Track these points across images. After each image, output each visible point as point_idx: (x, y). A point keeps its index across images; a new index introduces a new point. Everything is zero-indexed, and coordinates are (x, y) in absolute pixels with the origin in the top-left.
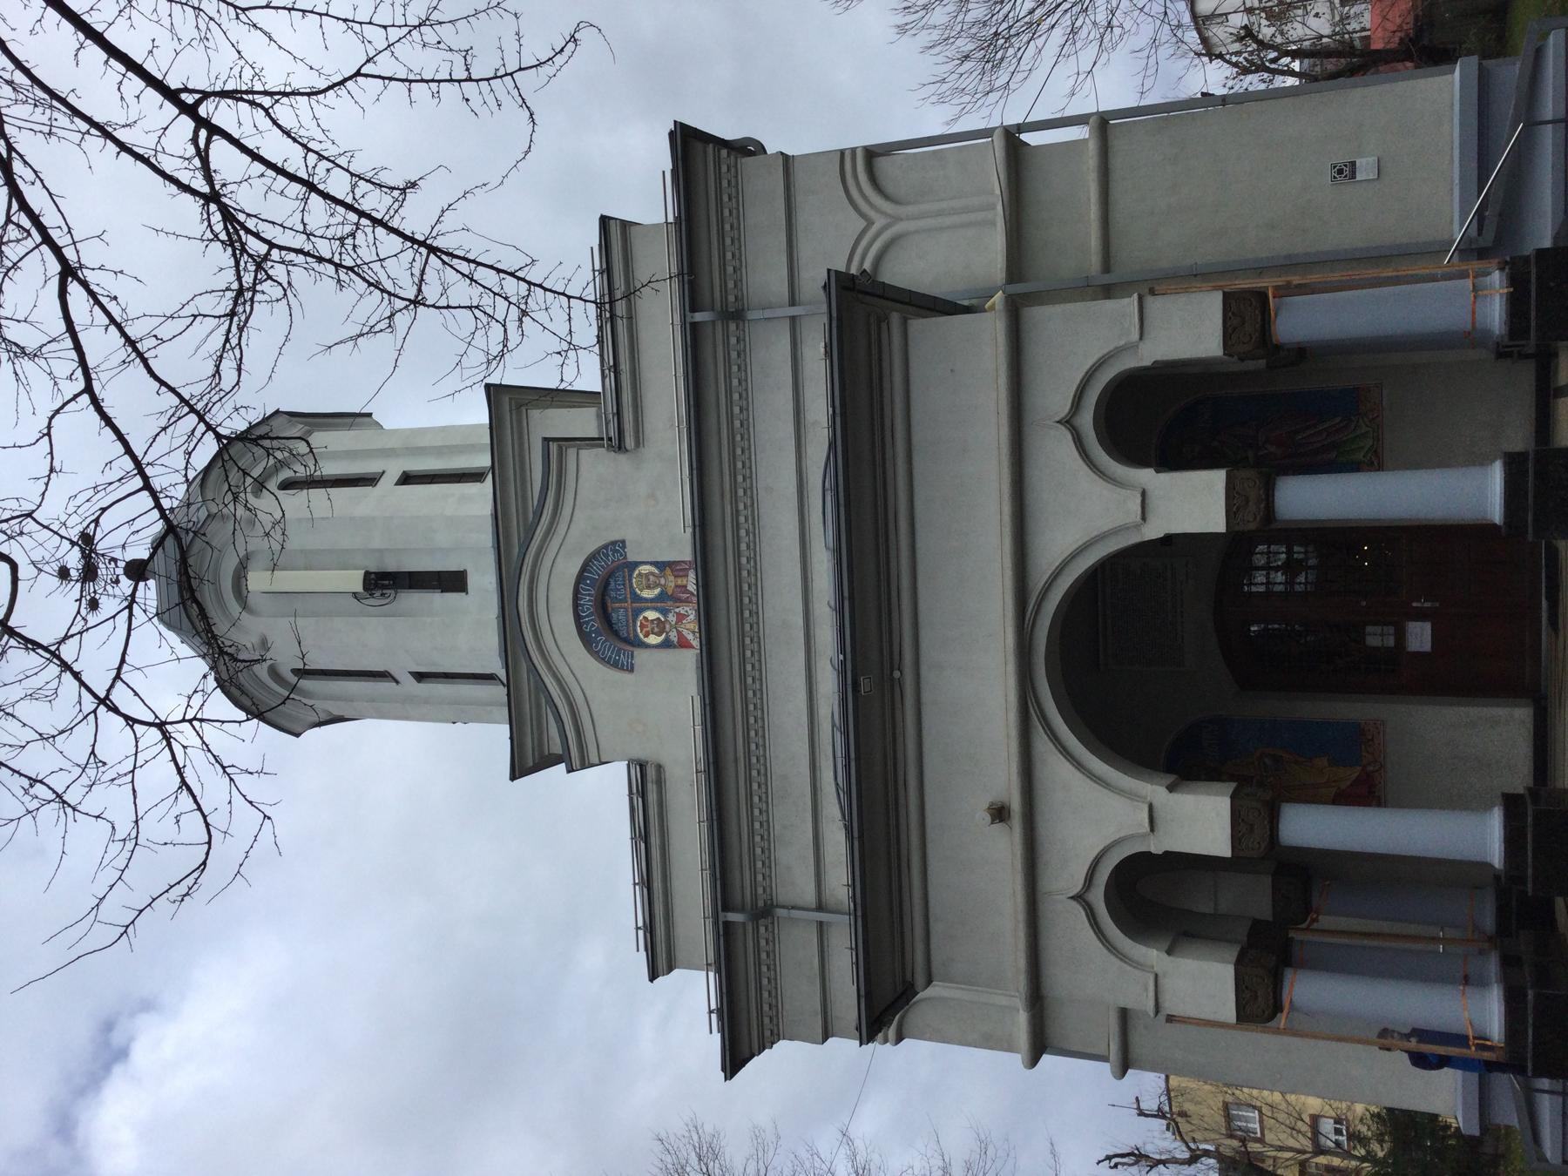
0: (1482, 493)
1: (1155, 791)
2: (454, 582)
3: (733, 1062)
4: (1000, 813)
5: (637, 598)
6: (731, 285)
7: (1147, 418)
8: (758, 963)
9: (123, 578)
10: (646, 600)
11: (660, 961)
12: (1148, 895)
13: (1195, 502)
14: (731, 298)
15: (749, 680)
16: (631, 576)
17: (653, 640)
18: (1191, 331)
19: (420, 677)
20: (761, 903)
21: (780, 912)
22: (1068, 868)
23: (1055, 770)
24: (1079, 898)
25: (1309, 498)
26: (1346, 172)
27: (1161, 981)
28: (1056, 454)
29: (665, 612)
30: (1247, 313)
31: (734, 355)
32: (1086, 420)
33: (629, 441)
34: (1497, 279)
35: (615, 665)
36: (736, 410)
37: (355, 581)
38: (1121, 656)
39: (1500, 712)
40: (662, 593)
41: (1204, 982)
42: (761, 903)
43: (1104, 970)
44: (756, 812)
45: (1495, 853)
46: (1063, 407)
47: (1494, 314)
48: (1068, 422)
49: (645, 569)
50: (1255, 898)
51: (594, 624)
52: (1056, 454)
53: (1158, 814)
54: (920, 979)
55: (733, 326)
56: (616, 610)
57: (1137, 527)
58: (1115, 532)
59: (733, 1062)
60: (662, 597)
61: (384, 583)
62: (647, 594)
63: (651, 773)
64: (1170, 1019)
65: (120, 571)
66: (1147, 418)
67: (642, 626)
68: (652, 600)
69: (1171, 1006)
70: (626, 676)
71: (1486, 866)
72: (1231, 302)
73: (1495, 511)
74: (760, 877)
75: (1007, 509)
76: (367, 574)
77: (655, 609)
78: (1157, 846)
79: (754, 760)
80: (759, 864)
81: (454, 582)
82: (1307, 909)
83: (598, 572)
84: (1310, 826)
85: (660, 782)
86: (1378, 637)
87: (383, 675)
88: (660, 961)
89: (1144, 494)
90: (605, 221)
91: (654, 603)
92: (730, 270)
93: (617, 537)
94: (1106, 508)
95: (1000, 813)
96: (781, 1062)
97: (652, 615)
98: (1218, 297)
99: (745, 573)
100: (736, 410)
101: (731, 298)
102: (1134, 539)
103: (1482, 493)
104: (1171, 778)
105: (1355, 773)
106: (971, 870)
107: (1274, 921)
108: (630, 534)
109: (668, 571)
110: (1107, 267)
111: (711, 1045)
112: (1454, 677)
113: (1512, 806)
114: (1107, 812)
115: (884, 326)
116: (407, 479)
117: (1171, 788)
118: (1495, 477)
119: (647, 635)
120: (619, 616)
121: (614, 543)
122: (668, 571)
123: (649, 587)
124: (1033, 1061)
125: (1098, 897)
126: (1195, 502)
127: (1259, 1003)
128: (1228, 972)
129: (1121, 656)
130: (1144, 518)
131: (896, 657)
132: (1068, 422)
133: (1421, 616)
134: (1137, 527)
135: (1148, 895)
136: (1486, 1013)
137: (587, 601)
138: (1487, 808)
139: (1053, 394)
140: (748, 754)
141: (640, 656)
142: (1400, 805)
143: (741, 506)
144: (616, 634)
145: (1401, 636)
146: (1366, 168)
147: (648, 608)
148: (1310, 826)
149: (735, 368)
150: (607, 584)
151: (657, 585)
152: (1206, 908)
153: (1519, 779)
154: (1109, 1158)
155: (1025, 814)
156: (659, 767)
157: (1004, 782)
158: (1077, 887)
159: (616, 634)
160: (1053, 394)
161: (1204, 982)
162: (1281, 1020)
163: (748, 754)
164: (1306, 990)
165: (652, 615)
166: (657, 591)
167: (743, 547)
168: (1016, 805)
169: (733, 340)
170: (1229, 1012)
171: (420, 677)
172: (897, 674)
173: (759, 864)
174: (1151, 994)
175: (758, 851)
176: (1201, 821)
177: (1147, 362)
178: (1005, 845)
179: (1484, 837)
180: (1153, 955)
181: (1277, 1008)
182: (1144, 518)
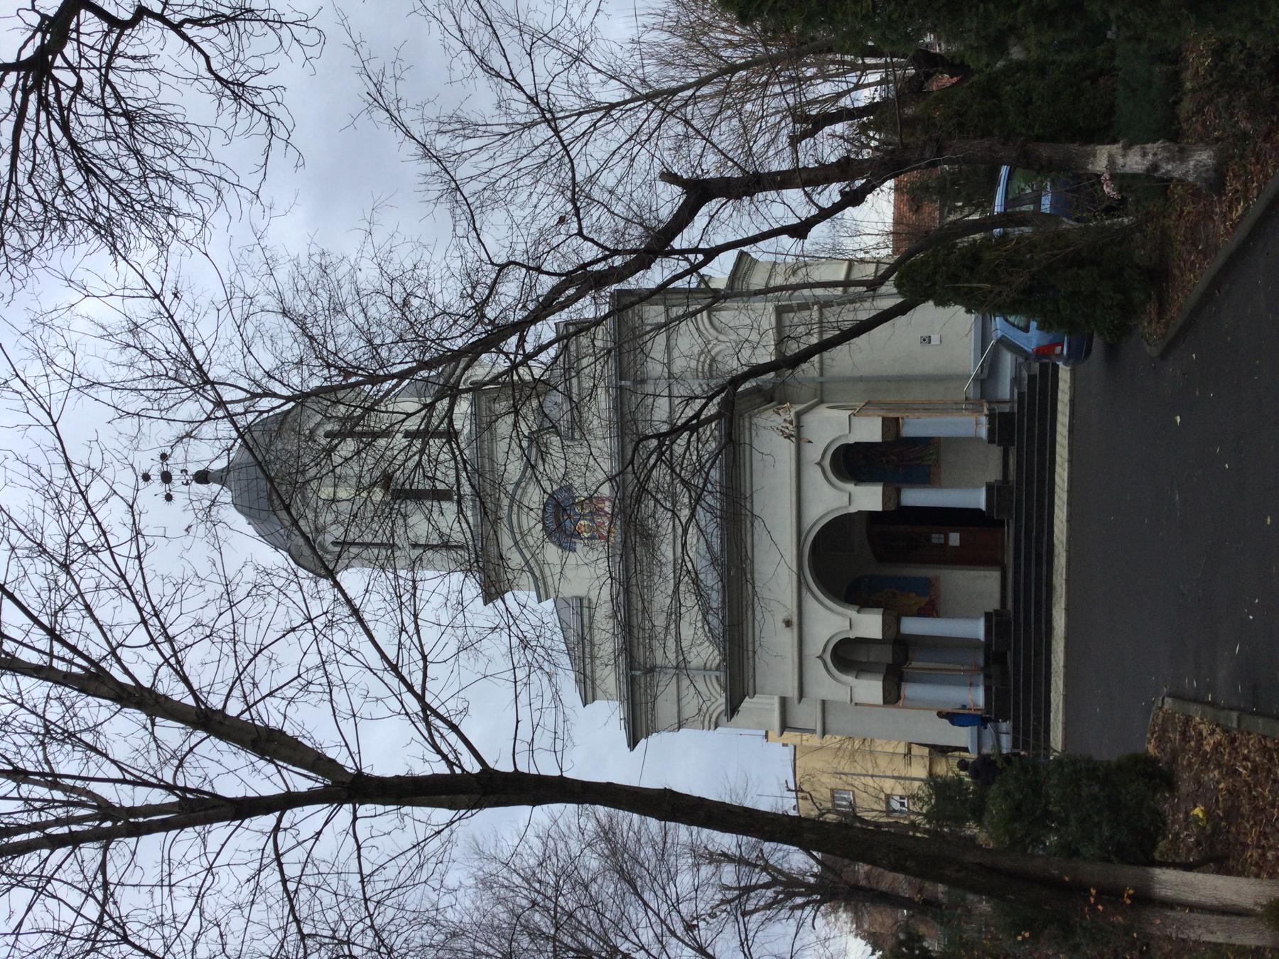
0: (978, 499)
1: (852, 613)
3: (633, 742)
7: (851, 462)
11: (588, 694)
12: (847, 656)
13: (869, 498)
18: (869, 430)
23: (811, 605)
24: (820, 657)
25: (914, 497)
26: (927, 340)
28: (814, 477)
30: (891, 425)
32: (827, 463)
34: (984, 420)
38: (837, 560)
39: (987, 573)
43: (829, 685)
47: (983, 432)
48: (819, 464)
50: (886, 656)
52: (814, 477)
54: (751, 692)
58: (837, 509)
59: (633, 742)
63: (586, 603)
66: (851, 462)
69: (856, 700)
72: (884, 420)
73: (983, 506)
78: (852, 636)
82: (907, 659)
84: (913, 626)
86: (937, 539)
88: (588, 694)
94: (834, 498)
96: (653, 743)
98: (880, 419)
105: (927, 599)
106: (775, 646)
107: (897, 663)
110: (821, 375)
111: (622, 736)
112: (967, 558)
113: (988, 616)
114: (832, 622)
124: (782, 734)
125: (828, 657)
126: (869, 498)
127: (892, 696)
128: (880, 684)
129: (837, 560)
132: (819, 464)
135: (847, 656)
136: (976, 697)
138: (978, 618)
139: (814, 453)
142: (948, 617)
145: (947, 539)
146: (935, 340)
148: (913, 626)
152: (864, 660)
153: (994, 604)
155: (798, 624)
160: (814, 453)
161: (870, 689)
162: (901, 703)
164: (909, 690)
168: (795, 620)
170: (881, 701)
176: (870, 625)
177: (852, 442)
179: (977, 629)
180: (850, 679)
181: (899, 698)
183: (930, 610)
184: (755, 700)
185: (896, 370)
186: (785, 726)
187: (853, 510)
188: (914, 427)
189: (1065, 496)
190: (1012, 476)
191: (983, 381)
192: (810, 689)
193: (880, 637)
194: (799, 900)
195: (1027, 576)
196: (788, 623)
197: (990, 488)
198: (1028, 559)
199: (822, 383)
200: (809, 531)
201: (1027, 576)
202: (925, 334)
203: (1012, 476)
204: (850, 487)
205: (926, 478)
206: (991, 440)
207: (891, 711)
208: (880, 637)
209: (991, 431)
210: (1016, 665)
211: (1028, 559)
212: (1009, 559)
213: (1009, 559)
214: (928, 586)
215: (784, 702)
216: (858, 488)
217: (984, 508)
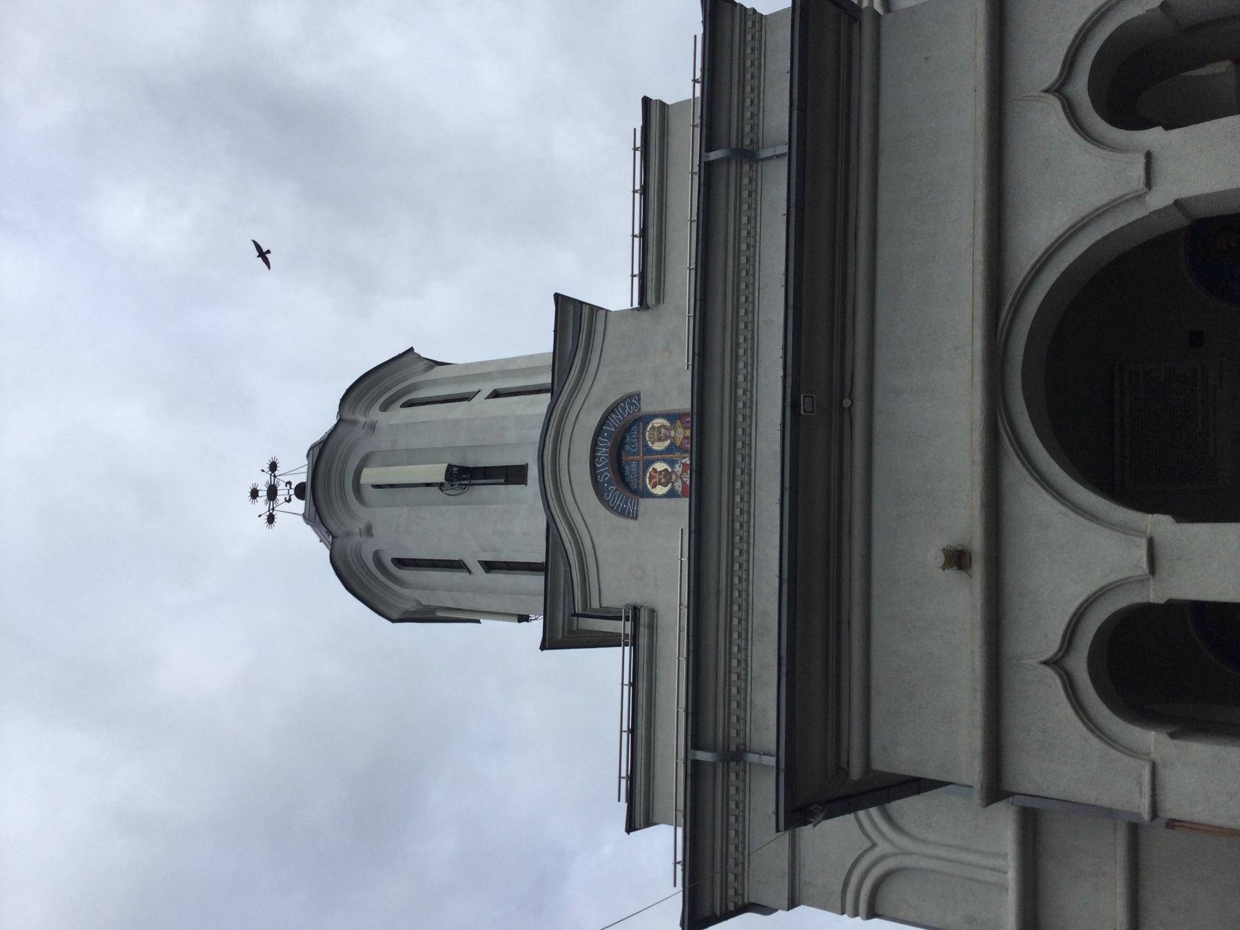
2: (515, 475)
4: (957, 559)
5: (650, 451)
6: (747, 128)
8: (726, 812)
9: (294, 498)
10: (657, 452)
14: (747, 142)
15: (737, 512)
16: (645, 429)
17: (660, 490)
19: (489, 566)
20: (733, 748)
21: (752, 758)
22: (1040, 630)
24: (1055, 663)
27: (1163, 773)
28: (1044, 127)
29: (672, 463)
31: (745, 194)
32: (1080, 87)
33: (651, 298)
35: (623, 513)
36: (744, 247)
37: (437, 473)
40: (672, 444)
42: (733, 748)
44: (735, 649)
46: (1052, 71)
48: (1059, 89)
49: (658, 422)
51: (607, 474)
53: (1162, 552)
55: (746, 167)
56: (629, 463)
57: (1139, 197)
60: (669, 450)
61: (463, 476)
62: (658, 446)
63: (644, 618)
64: (1172, 824)
65: (292, 492)
67: (651, 477)
68: (661, 452)
69: (1173, 807)
70: (631, 523)
74: (734, 719)
75: (981, 196)
76: (450, 467)
77: (664, 460)
79: (736, 594)
80: (734, 705)
81: (515, 475)
83: (616, 422)
85: (652, 627)
87: (457, 565)
89: (1149, 156)
90: (646, 101)
91: (665, 455)
92: (748, 115)
93: (631, 389)
95: (957, 559)
97: (660, 466)
99: (740, 405)
100: (744, 247)
101: (747, 142)
102: (1136, 213)
106: (925, 637)
108: (644, 385)
109: (678, 423)
114: (1091, 554)
115: (856, 26)
116: (496, 394)
119: (654, 487)
120: (631, 468)
121: (631, 396)
122: (678, 423)
123: (660, 440)
125: (1079, 664)
130: (1149, 182)
131: (848, 387)
132: (1059, 89)
134: (1139, 197)
137: (603, 453)
140: (730, 585)
141: (645, 503)
143: (741, 340)
144: (627, 486)
147: (658, 460)
149: (745, 207)
150: (624, 438)
151: (667, 437)
155: (991, 560)
156: (652, 612)
157: (964, 522)
159: (627, 486)
163: (730, 585)
165: (660, 466)
166: (667, 443)
167: (741, 378)
168: (977, 545)
169: (746, 181)
171: (489, 566)
172: (847, 403)
173: (734, 705)
174: (1147, 789)
175: (734, 690)
178: (963, 598)
180: (1151, 739)
182: (1149, 182)
216: (1175, 133)
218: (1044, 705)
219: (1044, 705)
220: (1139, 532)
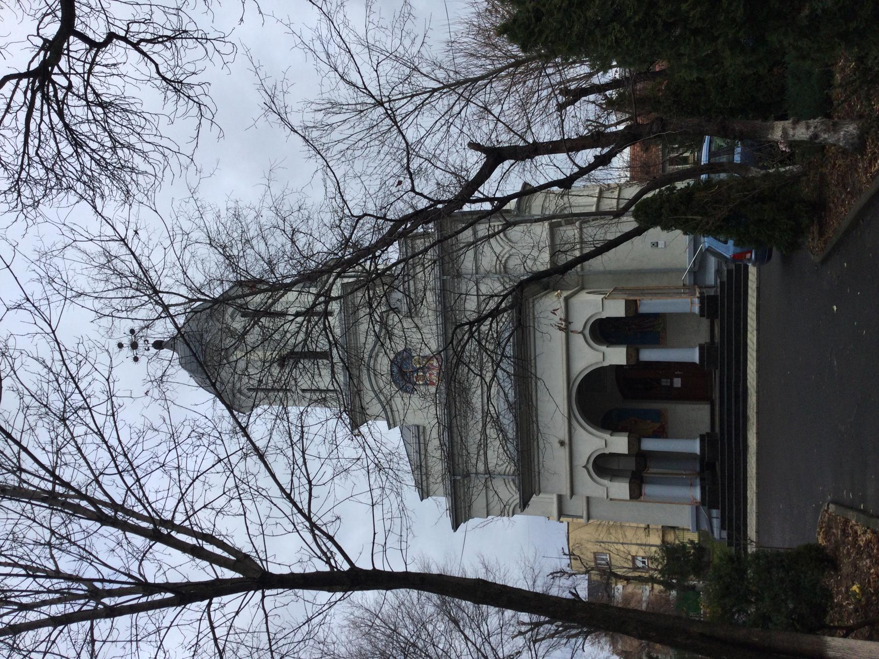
0: (694, 356)
1: (607, 436)
3: (456, 526)
7: (603, 331)
11: (424, 493)
12: (603, 466)
13: (617, 356)
18: (616, 309)
25: (649, 355)
28: (578, 341)
30: (631, 305)
34: (697, 301)
38: (597, 399)
39: (701, 406)
41: (621, 489)
43: (591, 486)
45: (697, 450)
47: (696, 309)
50: (631, 465)
52: (578, 341)
58: (597, 363)
59: (456, 526)
64: (611, 499)
66: (603, 331)
69: (611, 496)
71: (696, 454)
72: (626, 301)
73: (697, 360)
78: (607, 451)
84: (649, 445)
85: (424, 432)
86: (665, 382)
88: (424, 493)
94: (591, 357)
98: (623, 302)
102: (600, 365)
103: (694, 356)
104: (610, 432)
105: (658, 425)
106: (554, 461)
107: (638, 471)
111: (447, 521)
112: (689, 395)
113: (702, 438)
114: (592, 442)
117: (611, 435)
118: (697, 351)
125: (590, 466)
126: (617, 356)
127: (636, 494)
129: (597, 399)
133: (677, 376)
135: (603, 466)
138: (694, 438)
145: (672, 383)
148: (649, 445)
152: (616, 467)
153: (705, 428)
154: (552, 574)
155: (569, 444)
156: (424, 428)
157: (563, 434)
158: (584, 464)
161: (621, 489)
162: (642, 498)
164: (649, 490)
168: (567, 441)
170: (628, 498)
176: (619, 444)
178: (564, 453)
179: (695, 447)
180: (606, 482)
181: (641, 495)
183: (661, 433)
184: (541, 495)
185: (634, 265)
186: (561, 514)
187: (606, 364)
188: (649, 305)
189: (755, 354)
190: (717, 339)
191: (695, 272)
192: (579, 488)
193: (626, 452)
194: (574, 632)
195: (729, 409)
196: (562, 443)
197: (702, 348)
198: (729, 399)
199: (583, 276)
200: (576, 379)
201: (729, 409)
202: (654, 241)
203: (717, 339)
204: (604, 348)
205: (657, 340)
206: (702, 314)
207: (635, 504)
208: (626, 452)
209: (702, 309)
210: (723, 471)
211: (729, 399)
212: (716, 395)
213: (716, 395)
214: (659, 415)
215: (560, 498)
217: (697, 360)
218: (583, 476)
219: (583, 476)
220: (602, 438)
